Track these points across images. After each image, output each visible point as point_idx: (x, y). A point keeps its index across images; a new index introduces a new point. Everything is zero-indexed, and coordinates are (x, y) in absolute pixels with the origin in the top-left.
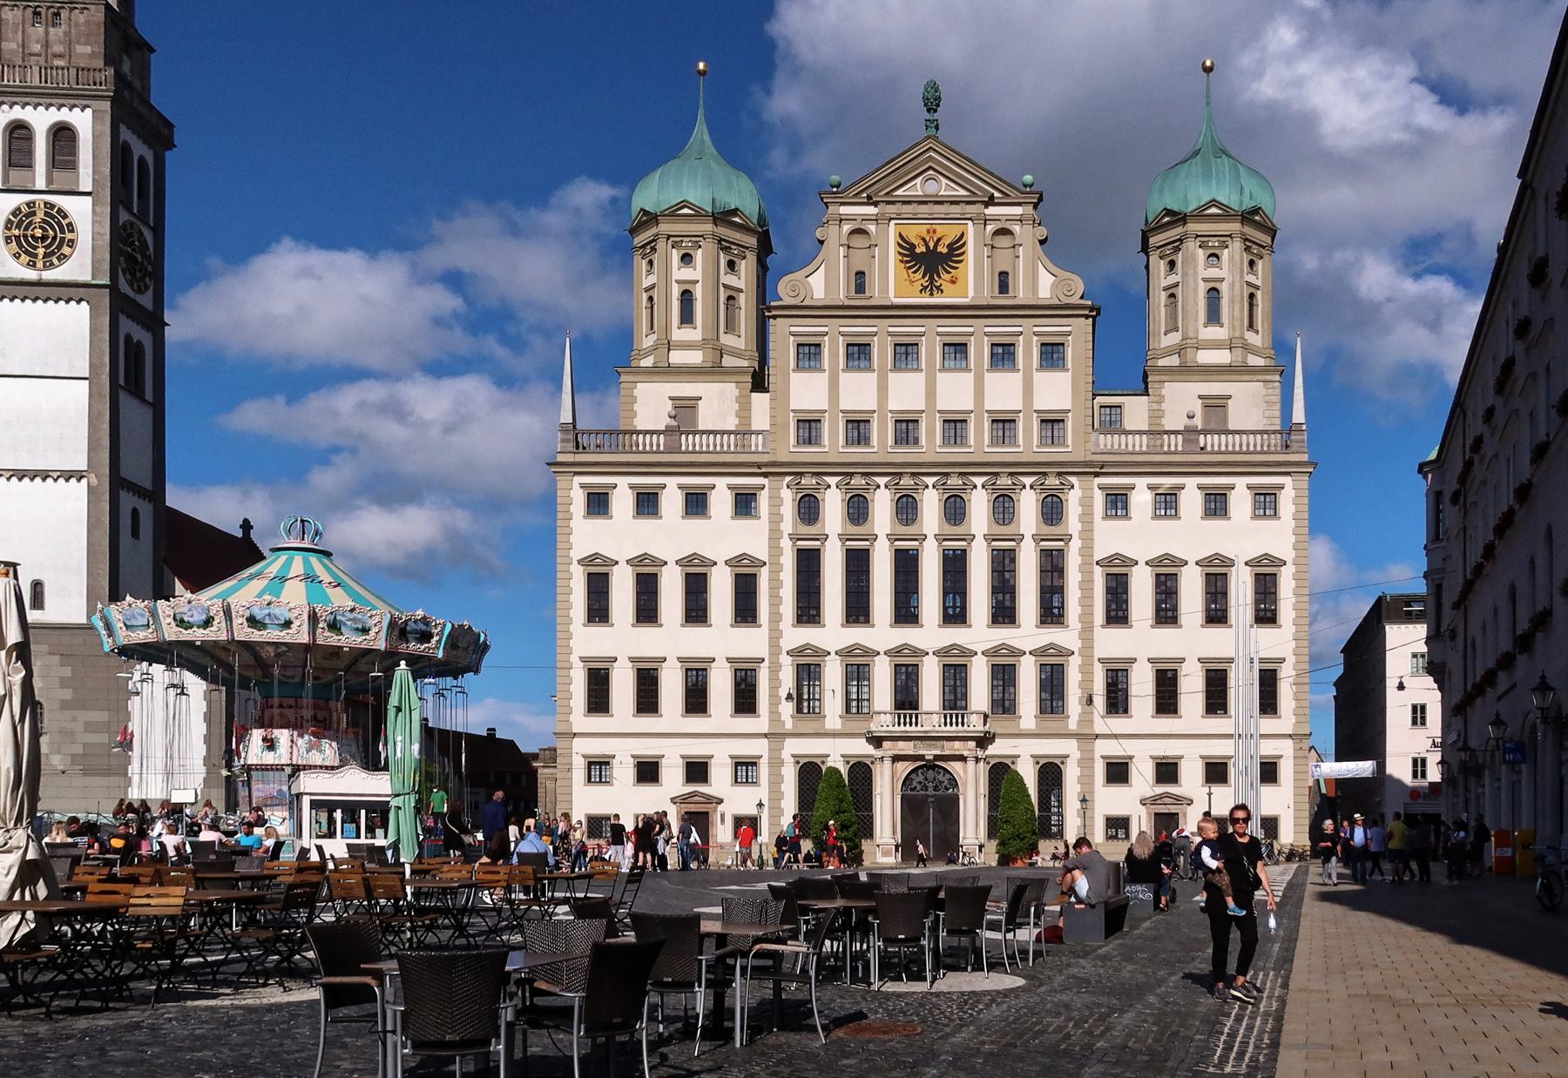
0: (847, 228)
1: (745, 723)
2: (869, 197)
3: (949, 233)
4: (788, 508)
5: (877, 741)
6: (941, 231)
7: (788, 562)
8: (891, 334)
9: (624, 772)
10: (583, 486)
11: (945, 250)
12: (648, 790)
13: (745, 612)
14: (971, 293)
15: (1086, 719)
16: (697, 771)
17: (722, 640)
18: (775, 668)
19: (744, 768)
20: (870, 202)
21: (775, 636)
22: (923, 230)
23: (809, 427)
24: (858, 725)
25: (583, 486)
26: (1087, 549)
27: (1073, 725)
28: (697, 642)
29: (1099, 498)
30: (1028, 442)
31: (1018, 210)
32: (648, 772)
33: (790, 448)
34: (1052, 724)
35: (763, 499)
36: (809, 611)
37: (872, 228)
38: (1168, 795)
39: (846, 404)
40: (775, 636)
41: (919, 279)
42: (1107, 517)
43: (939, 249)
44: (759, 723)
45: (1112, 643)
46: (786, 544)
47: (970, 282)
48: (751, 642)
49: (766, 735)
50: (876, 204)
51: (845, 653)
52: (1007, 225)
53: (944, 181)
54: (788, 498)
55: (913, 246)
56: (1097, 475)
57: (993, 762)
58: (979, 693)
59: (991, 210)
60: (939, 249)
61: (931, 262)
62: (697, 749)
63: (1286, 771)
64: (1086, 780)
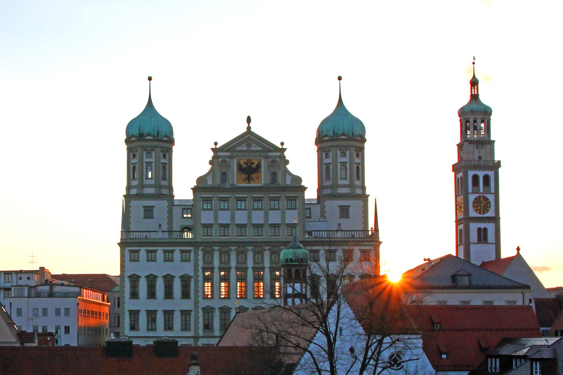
0: (220, 160)
3: (256, 162)
4: (200, 257)
6: (253, 161)
10: (129, 250)
14: (263, 183)
18: (197, 312)
20: (228, 151)
21: (196, 303)
22: (245, 161)
28: (169, 305)
35: (192, 254)
39: (220, 221)
40: (196, 303)
50: (229, 152)
51: (221, 309)
53: (253, 144)
54: (200, 253)
59: (271, 154)
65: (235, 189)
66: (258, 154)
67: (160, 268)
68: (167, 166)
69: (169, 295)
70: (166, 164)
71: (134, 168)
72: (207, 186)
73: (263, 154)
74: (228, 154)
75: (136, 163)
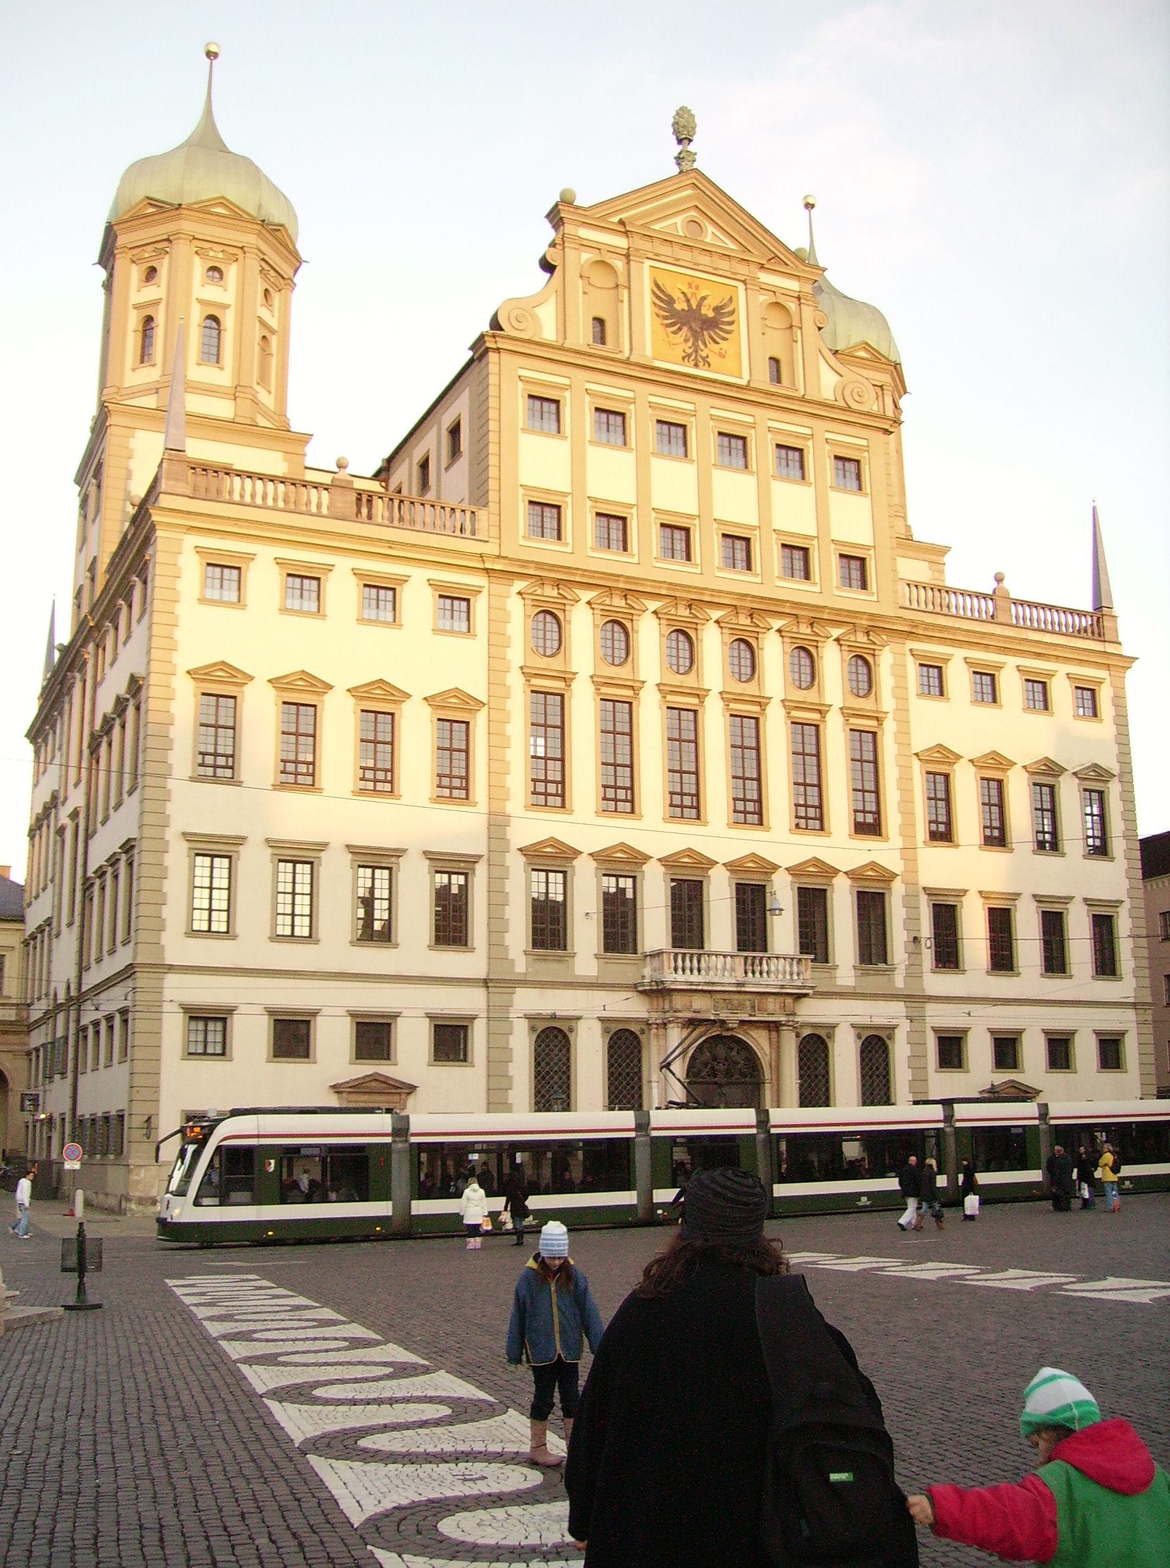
0: (586, 256)
1: (451, 962)
2: (621, 222)
5: (658, 992)
7: (518, 705)
8: (651, 405)
9: (252, 1034)
10: (199, 550)
11: (711, 314)
12: (291, 1069)
13: (454, 784)
15: (913, 972)
16: (373, 1036)
17: (417, 820)
19: (450, 1040)
20: (623, 228)
21: (497, 824)
23: (547, 511)
24: (623, 968)
25: (199, 550)
26: (903, 735)
27: (899, 981)
28: (377, 823)
29: (912, 667)
30: (827, 587)
31: (793, 285)
32: (292, 1036)
33: (519, 539)
34: (873, 983)
35: (480, 606)
36: (551, 789)
37: (619, 264)
38: (1013, 1084)
40: (497, 824)
41: (680, 341)
42: (920, 695)
43: (704, 311)
44: (469, 963)
45: (940, 868)
46: (516, 682)
47: (741, 356)
48: (459, 828)
49: (486, 983)
50: (626, 233)
52: (782, 300)
53: (710, 228)
54: (516, 608)
55: (670, 301)
56: (910, 635)
57: (806, 1032)
58: (783, 932)
59: (765, 278)
60: (704, 311)
61: (700, 324)
62: (375, 999)
63: (1131, 1050)
64: (916, 1059)
65: (647, 374)
66: (723, 264)
67: (342, 647)
68: (274, 340)
69: (379, 778)
70: (273, 332)
71: (149, 319)
72: (536, 339)
73: (742, 269)
74: (621, 242)
75: (156, 303)
